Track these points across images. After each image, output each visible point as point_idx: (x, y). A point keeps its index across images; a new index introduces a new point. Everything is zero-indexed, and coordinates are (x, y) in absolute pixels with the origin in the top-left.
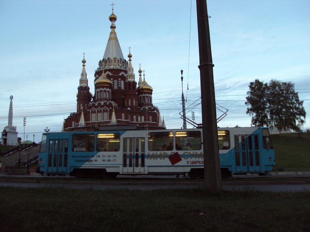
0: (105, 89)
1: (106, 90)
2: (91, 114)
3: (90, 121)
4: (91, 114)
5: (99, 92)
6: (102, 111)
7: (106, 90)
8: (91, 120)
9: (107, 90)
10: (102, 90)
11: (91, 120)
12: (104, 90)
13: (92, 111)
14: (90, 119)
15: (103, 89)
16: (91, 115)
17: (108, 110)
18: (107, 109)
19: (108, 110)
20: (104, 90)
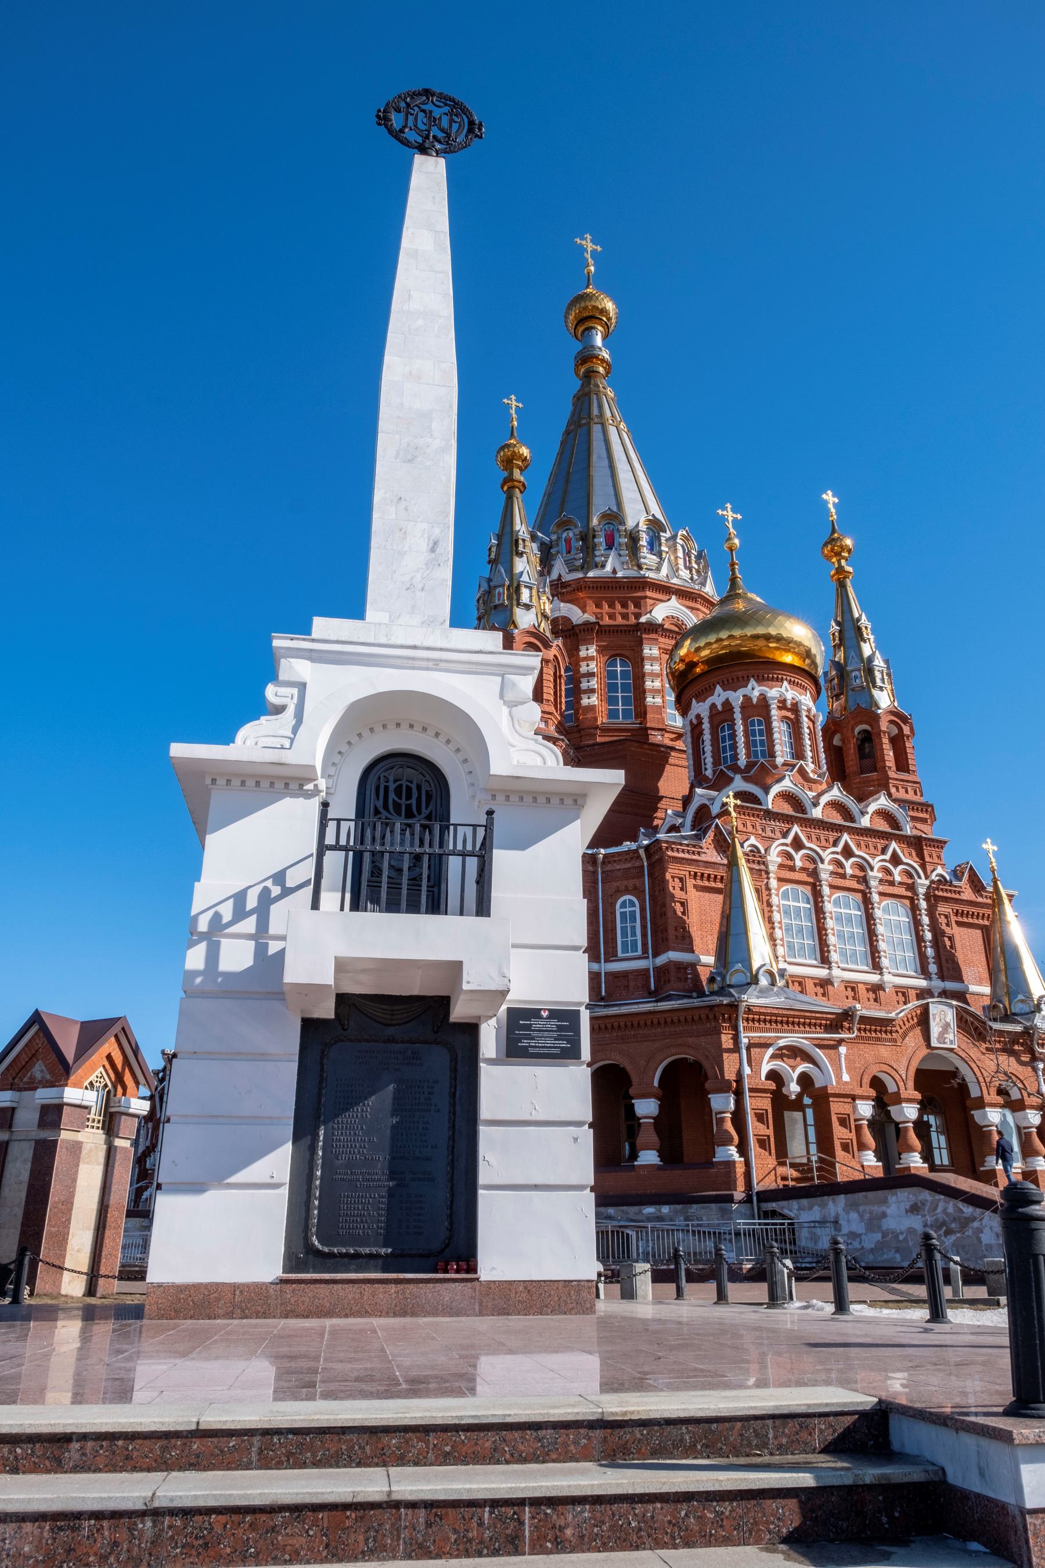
5: (706, 726)
9: (773, 693)
10: (727, 704)
12: (747, 698)
15: (736, 698)
20: (747, 698)
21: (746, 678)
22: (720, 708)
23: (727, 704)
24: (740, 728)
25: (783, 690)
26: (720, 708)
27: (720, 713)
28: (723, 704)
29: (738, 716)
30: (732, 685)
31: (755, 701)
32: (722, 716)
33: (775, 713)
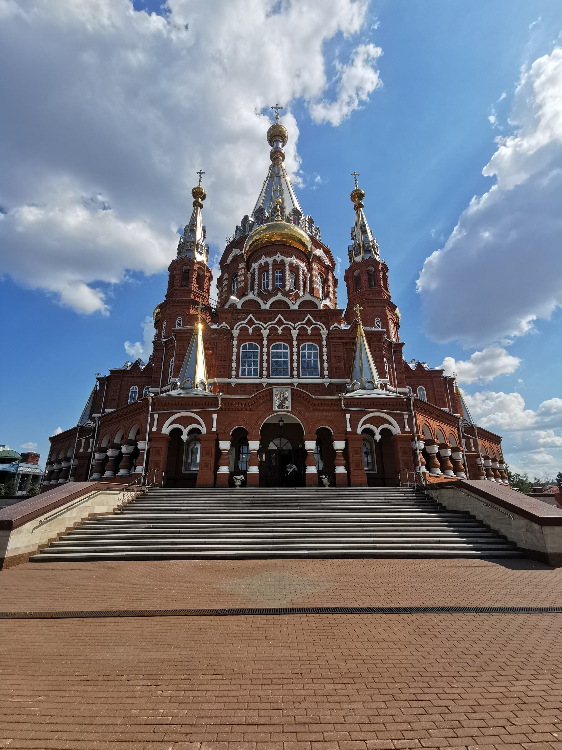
0: (279, 257)
1: (282, 261)
2: (235, 342)
3: (230, 377)
4: (235, 342)
5: (257, 273)
6: (295, 336)
7: (282, 261)
8: (234, 373)
9: (287, 260)
10: (266, 263)
11: (234, 373)
12: (275, 261)
13: (244, 330)
14: (231, 369)
15: (270, 260)
16: (235, 350)
17: (324, 333)
18: (316, 330)
19: (324, 333)
20: (275, 261)
21: (275, 252)
22: (263, 264)
23: (266, 263)
24: (270, 273)
25: (293, 258)
26: (263, 264)
27: (263, 267)
28: (265, 263)
29: (270, 268)
30: (268, 255)
31: (279, 262)
32: (264, 269)
33: (287, 267)
